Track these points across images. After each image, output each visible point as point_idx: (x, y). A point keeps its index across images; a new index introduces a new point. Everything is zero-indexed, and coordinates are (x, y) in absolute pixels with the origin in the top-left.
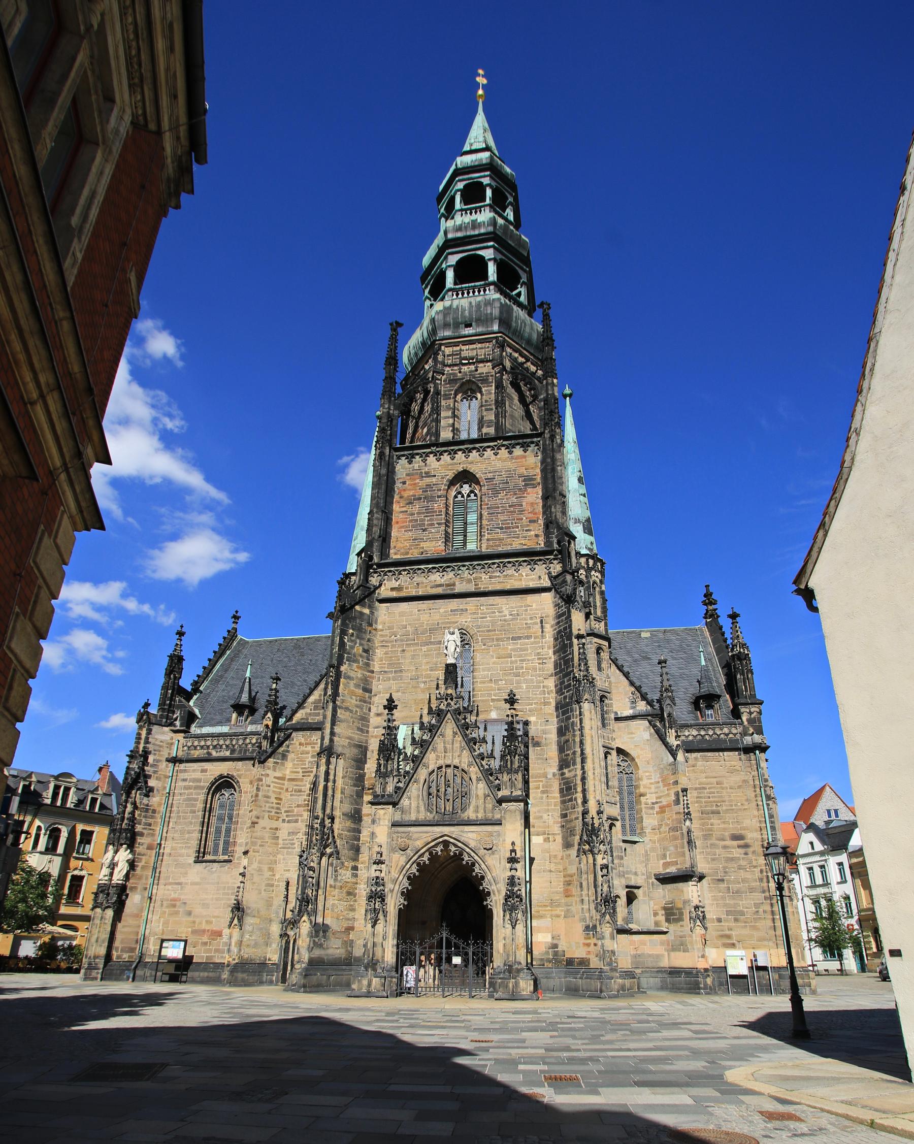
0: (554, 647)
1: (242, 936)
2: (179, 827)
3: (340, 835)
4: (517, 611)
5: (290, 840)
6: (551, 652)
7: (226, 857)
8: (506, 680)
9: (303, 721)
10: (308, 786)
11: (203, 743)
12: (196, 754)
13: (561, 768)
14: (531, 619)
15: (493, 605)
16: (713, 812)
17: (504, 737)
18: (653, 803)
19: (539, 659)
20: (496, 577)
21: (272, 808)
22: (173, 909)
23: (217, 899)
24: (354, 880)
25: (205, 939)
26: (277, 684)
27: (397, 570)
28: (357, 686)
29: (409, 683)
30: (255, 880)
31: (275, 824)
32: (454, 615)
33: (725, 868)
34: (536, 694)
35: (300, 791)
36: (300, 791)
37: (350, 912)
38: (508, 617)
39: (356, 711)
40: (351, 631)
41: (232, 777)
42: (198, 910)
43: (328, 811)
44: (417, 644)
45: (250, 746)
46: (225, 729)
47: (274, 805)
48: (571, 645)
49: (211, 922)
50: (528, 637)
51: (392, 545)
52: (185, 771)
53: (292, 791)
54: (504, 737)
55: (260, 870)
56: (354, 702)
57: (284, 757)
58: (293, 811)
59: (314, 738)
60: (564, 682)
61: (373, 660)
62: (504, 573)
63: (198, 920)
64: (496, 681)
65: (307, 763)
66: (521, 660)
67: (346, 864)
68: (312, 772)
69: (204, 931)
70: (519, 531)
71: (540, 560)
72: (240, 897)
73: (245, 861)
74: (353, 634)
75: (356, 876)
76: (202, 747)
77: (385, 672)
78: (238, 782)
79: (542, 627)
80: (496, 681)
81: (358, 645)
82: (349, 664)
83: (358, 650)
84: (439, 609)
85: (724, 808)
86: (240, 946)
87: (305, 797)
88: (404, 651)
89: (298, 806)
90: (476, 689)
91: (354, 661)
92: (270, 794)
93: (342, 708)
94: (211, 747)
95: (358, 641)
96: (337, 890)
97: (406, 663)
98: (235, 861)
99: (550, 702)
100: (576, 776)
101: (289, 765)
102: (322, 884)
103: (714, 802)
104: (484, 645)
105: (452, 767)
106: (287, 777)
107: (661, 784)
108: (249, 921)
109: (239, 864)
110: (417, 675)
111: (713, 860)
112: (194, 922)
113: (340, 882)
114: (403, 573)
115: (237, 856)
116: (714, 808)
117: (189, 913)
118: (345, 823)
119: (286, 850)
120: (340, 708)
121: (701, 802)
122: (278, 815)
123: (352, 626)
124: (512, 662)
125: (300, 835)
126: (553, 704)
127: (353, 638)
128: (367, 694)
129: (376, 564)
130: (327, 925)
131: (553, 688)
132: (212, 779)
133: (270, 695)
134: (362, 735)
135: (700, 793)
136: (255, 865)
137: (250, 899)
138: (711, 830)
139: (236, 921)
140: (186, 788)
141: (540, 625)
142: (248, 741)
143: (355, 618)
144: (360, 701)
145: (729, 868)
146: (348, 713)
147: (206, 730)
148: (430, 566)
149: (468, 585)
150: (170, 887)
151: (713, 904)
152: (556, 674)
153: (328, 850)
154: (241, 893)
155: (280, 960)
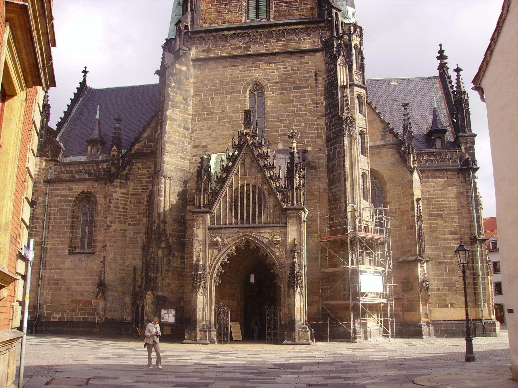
0: (325, 95)
1: (106, 304)
2: (55, 230)
3: (171, 235)
4: (298, 67)
5: (135, 238)
6: (322, 98)
7: (90, 251)
8: (289, 120)
9: (139, 151)
10: (146, 199)
11: (68, 169)
12: (64, 176)
13: (329, 184)
14: (308, 73)
15: (279, 62)
16: (438, 215)
17: (288, 163)
18: (396, 209)
19: (313, 104)
20: (281, 41)
21: (121, 215)
22: (57, 286)
23: (87, 279)
25: (81, 306)
26: (119, 124)
27: (206, 37)
28: (179, 126)
30: (112, 266)
31: (123, 227)
32: (250, 70)
33: (444, 254)
34: (312, 130)
35: (140, 202)
36: (140, 202)
38: (290, 72)
39: (179, 144)
40: (173, 84)
41: (91, 193)
42: (74, 287)
43: (162, 218)
44: (222, 93)
45: (102, 170)
46: (83, 158)
47: (122, 213)
48: (337, 92)
49: (83, 295)
50: (306, 87)
51: (202, 16)
52: (58, 189)
53: (134, 203)
54: (288, 163)
55: (115, 259)
56: (177, 137)
57: (127, 178)
58: (136, 217)
59: (148, 164)
61: (190, 106)
62: (288, 38)
63: (74, 294)
64: (282, 121)
65: (144, 182)
66: (300, 105)
67: (176, 254)
68: (148, 189)
69: (80, 300)
70: (299, 5)
71: (314, 28)
72: (102, 278)
73: (103, 254)
74: (174, 87)
75: (183, 263)
76: (68, 172)
77: (199, 114)
78: (95, 197)
79: (316, 79)
80: (282, 121)
81: (178, 95)
82: (173, 109)
83: (179, 98)
84: (239, 66)
85: (446, 212)
86: (105, 311)
87: (144, 207)
88: (213, 98)
89: (139, 213)
90: (267, 127)
91: (177, 107)
92: (119, 205)
94: (74, 172)
95: (179, 91)
96: (170, 273)
97: (215, 108)
98: (97, 253)
100: (340, 190)
101: (131, 184)
102: (160, 269)
103: (439, 208)
104: (273, 93)
105: (251, 185)
106: (130, 193)
107: (402, 195)
108: (109, 294)
109: (100, 255)
110: (224, 117)
111: (436, 248)
112: (72, 295)
114: (211, 38)
115: (98, 249)
116: (439, 212)
117: (69, 289)
118: (175, 226)
119: (132, 245)
121: (430, 208)
122: (125, 220)
123: (174, 80)
124: (294, 106)
125: (142, 234)
126: (324, 138)
127: (175, 90)
128: (187, 132)
129: (190, 32)
130: (165, 297)
131: (324, 126)
132: (77, 194)
133: (115, 133)
134: (184, 162)
135: (430, 202)
136: (111, 256)
137: (110, 277)
138: (435, 227)
139: (101, 294)
140: (59, 201)
141: (314, 78)
142: (100, 167)
143: (175, 75)
144: (182, 137)
145: (447, 254)
146: (173, 147)
147: (69, 159)
148: (232, 32)
149: (260, 48)
150: (53, 271)
151: (435, 279)
152: (326, 115)
153: (163, 245)
154: (103, 276)
155: (132, 318)
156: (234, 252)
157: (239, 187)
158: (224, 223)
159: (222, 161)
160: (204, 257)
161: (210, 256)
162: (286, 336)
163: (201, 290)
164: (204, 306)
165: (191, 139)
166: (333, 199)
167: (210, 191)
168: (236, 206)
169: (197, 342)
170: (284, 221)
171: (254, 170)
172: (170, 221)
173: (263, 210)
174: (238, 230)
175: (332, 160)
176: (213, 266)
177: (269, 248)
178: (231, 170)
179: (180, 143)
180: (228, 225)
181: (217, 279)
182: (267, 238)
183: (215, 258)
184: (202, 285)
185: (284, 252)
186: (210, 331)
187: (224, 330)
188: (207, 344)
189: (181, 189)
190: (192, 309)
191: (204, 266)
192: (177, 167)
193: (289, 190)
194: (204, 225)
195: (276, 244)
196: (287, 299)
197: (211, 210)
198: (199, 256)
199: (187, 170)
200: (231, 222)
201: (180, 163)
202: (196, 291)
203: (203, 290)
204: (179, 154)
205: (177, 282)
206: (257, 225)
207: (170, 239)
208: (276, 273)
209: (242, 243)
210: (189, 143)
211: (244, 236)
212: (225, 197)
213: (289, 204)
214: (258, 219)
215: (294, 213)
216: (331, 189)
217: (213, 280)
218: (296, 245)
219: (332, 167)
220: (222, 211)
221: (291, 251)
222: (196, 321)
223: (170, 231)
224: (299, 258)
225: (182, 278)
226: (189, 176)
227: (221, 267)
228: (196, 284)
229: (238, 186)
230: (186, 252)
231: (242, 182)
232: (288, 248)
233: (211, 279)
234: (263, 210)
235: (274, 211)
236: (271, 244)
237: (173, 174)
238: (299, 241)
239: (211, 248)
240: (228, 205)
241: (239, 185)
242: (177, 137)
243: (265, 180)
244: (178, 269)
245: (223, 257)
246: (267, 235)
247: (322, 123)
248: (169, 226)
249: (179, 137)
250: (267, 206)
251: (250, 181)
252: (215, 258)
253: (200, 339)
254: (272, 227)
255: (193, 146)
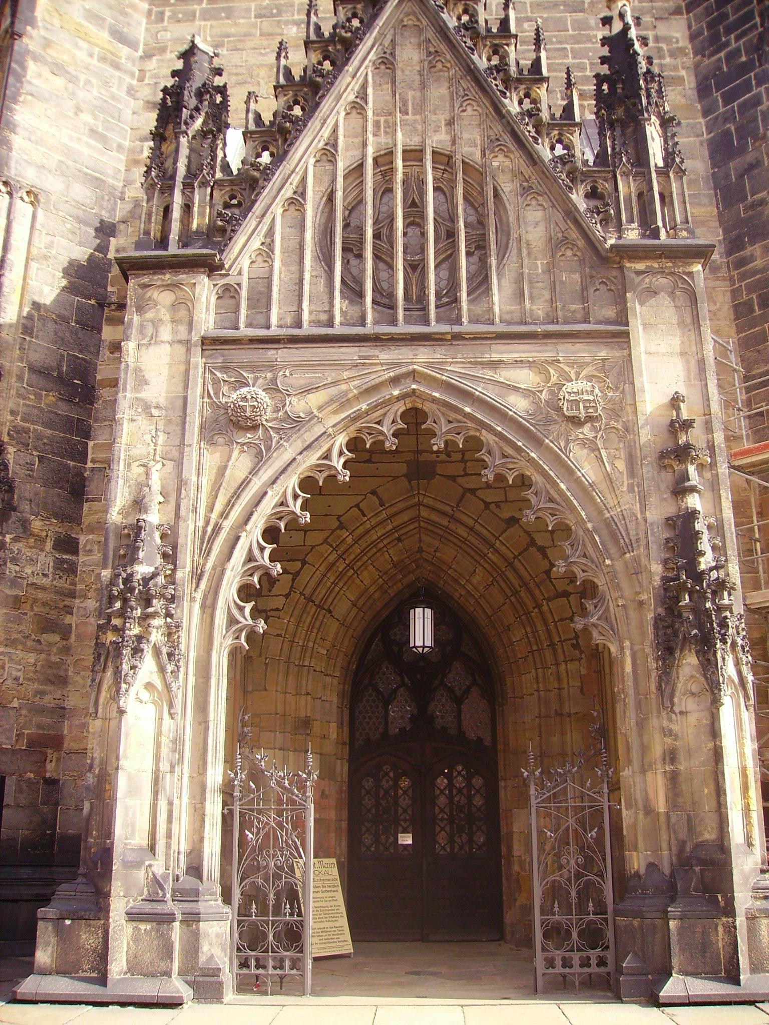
24: (63, 584)
29: (254, 26)
37: (50, 688)
39: (88, 82)
56: (82, 55)
60: (725, 16)
67: (37, 525)
93: (45, 63)
99: (681, 80)
113: (14, 583)
118: (38, 397)
120: (36, 59)
126: (690, 82)
128: (124, 51)
144: (103, 59)
146: (59, 82)
156: (338, 463)
157: (370, 161)
158: (289, 320)
159: (282, 48)
160: (172, 488)
161: (206, 483)
162: (675, 949)
163: (148, 667)
164: (164, 766)
165: (141, 80)
166: (759, 297)
167: (219, 175)
168: (353, 250)
169: (111, 991)
170: (610, 312)
171: (439, 92)
172: (15, 370)
173: (494, 262)
174: (366, 350)
175: (742, 150)
176: (223, 536)
177: (538, 443)
178: (332, 84)
179: (94, 81)
180: (307, 329)
181: (241, 609)
182: (527, 393)
183: (237, 494)
184: (156, 636)
185: (621, 465)
186: (192, 919)
187: (277, 911)
188: (173, 1004)
189: (81, 253)
190: (90, 779)
191: (170, 536)
192: (70, 163)
193: (625, 174)
194: (183, 329)
195: (576, 422)
196: (654, 722)
197: (221, 252)
198: (143, 485)
199: (114, 188)
200: (324, 317)
201: (86, 151)
202: (117, 672)
203: (162, 670)
204: (86, 117)
205: (31, 658)
206: (466, 326)
207: (11, 450)
208: (581, 576)
209: (388, 421)
210: (131, 91)
211: (395, 381)
212: (297, 202)
213: (633, 235)
214: (470, 302)
215: (662, 272)
216: (741, 263)
217: (220, 618)
218: (687, 425)
219: (741, 177)
220: (277, 264)
221: (663, 455)
222: (107, 853)
223: (13, 413)
224: (708, 495)
225: (57, 638)
226: (121, 210)
227: (269, 548)
228: (120, 631)
229: (364, 156)
230: (86, 520)
231: (384, 140)
232: (643, 439)
233: (209, 607)
234: (494, 262)
235: (550, 268)
236: (549, 421)
237: (52, 184)
238: (699, 408)
239: (212, 443)
240: (309, 235)
241: (370, 151)
242: (82, 55)
243: (498, 128)
244: (40, 595)
245: (278, 488)
246: (525, 378)
247: (678, 35)
248: (13, 392)
249: (91, 55)
250: (513, 245)
251: (424, 132)
252: (237, 494)
253: (133, 968)
254: (548, 335)
255: (148, 102)
